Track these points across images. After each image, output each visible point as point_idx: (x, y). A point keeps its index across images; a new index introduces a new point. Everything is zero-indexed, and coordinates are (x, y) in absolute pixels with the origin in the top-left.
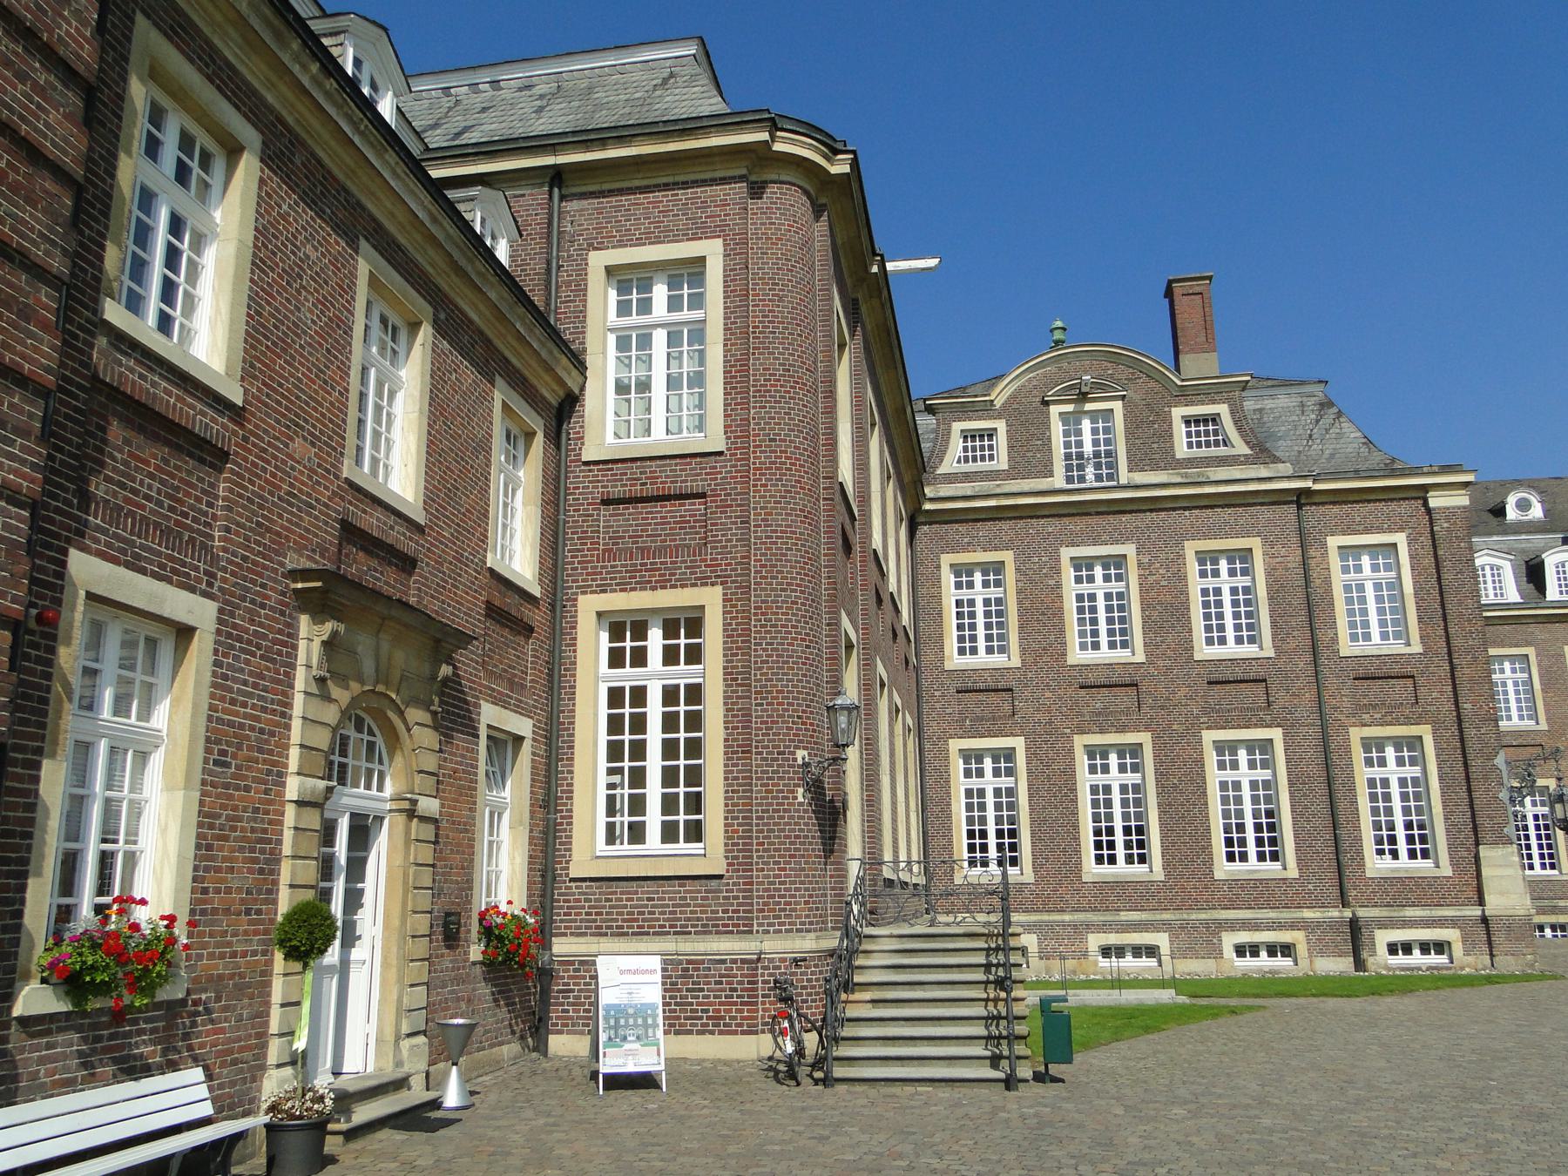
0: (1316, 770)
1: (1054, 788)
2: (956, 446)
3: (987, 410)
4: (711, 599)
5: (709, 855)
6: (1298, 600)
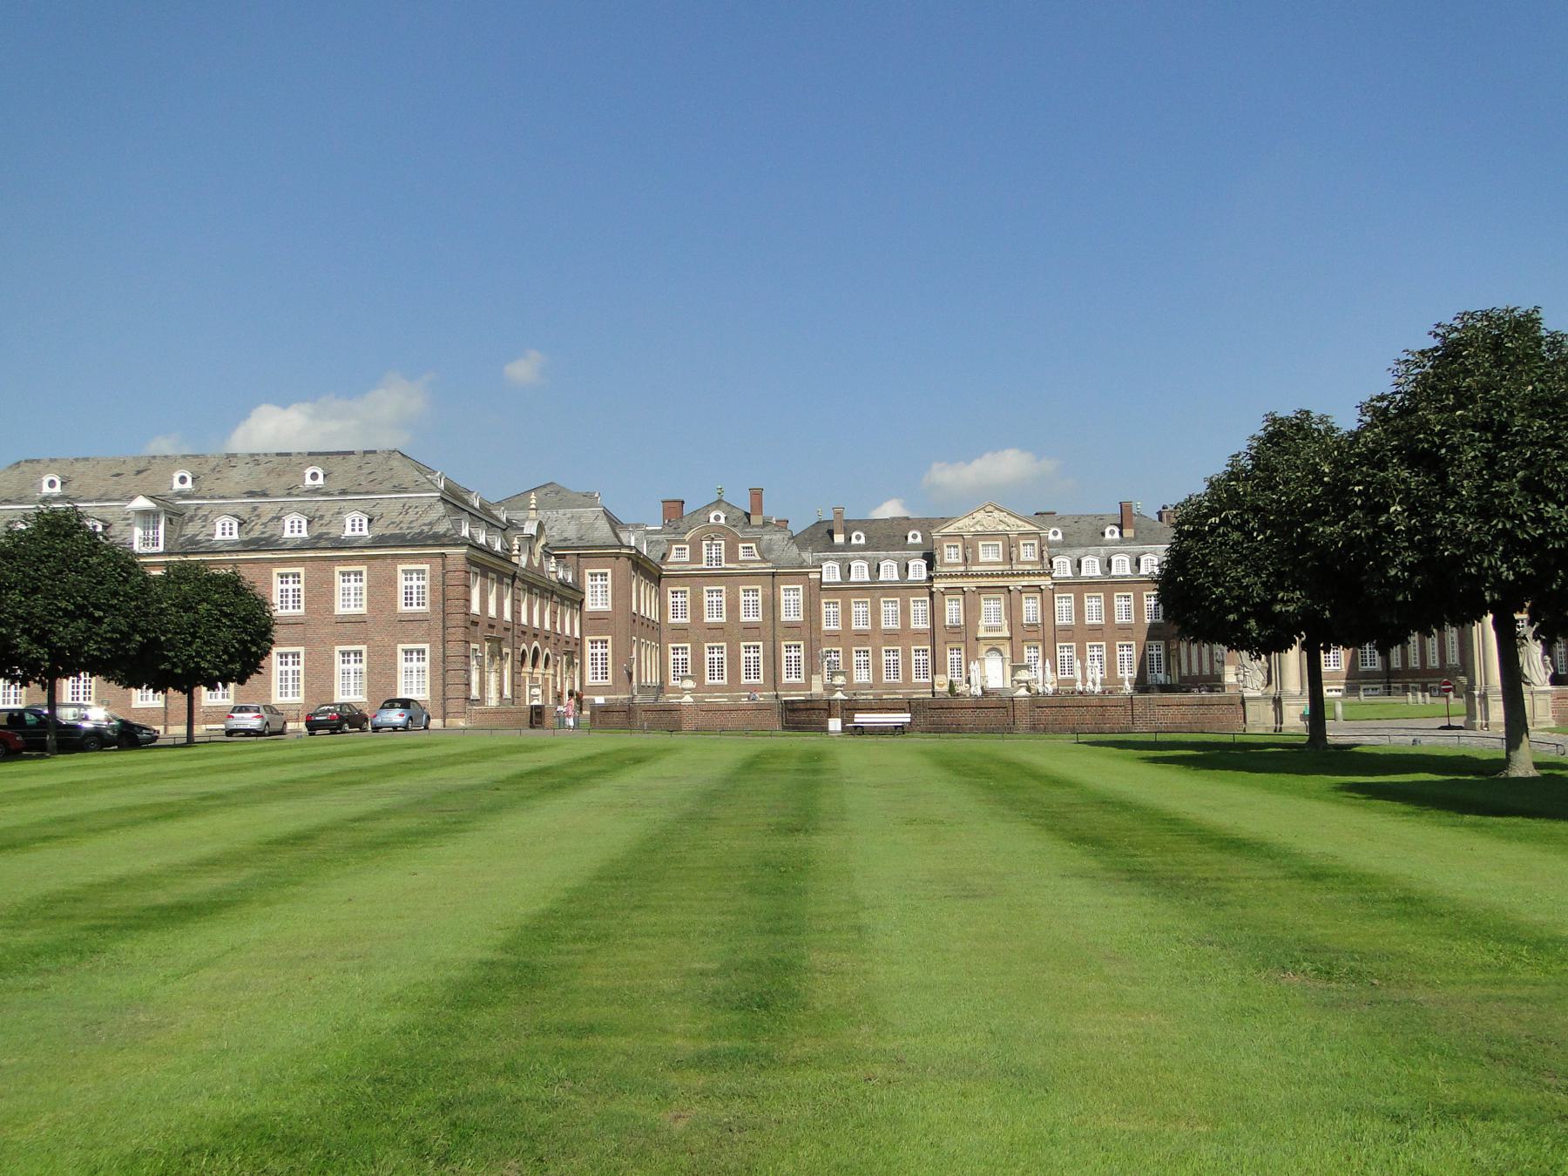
1: (698, 658)
2: (674, 552)
3: (683, 542)
4: (609, 638)
5: (609, 682)
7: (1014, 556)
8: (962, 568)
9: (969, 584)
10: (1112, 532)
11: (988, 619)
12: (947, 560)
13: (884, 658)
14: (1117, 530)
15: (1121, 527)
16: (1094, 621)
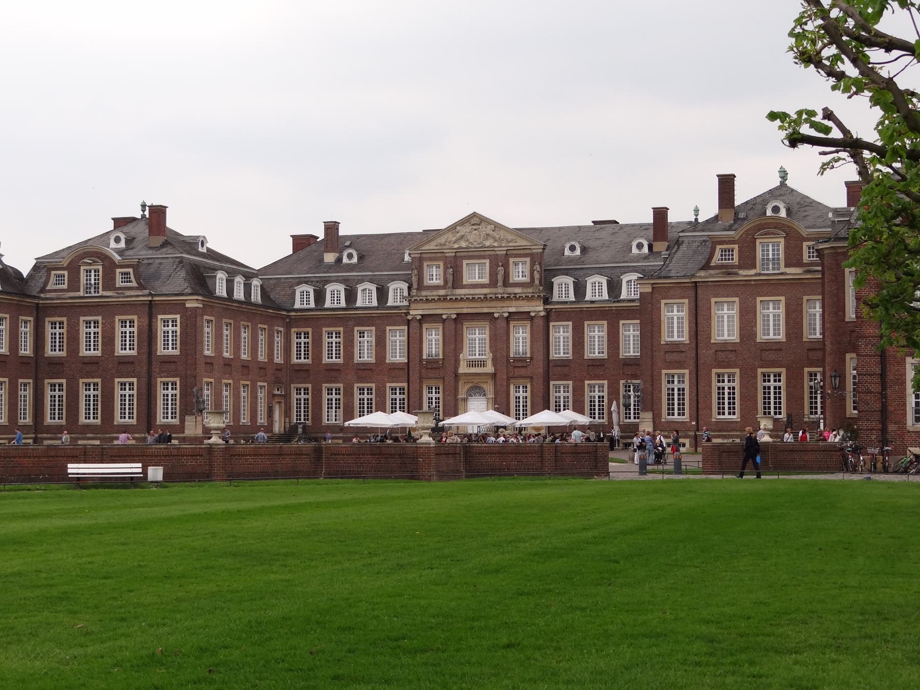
0: (144, 391)
2: (53, 279)
6: (145, 336)
7: (500, 277)
8: (442, 292)
9: (448, 311)
10: (640, 246)
13: (357, 396)
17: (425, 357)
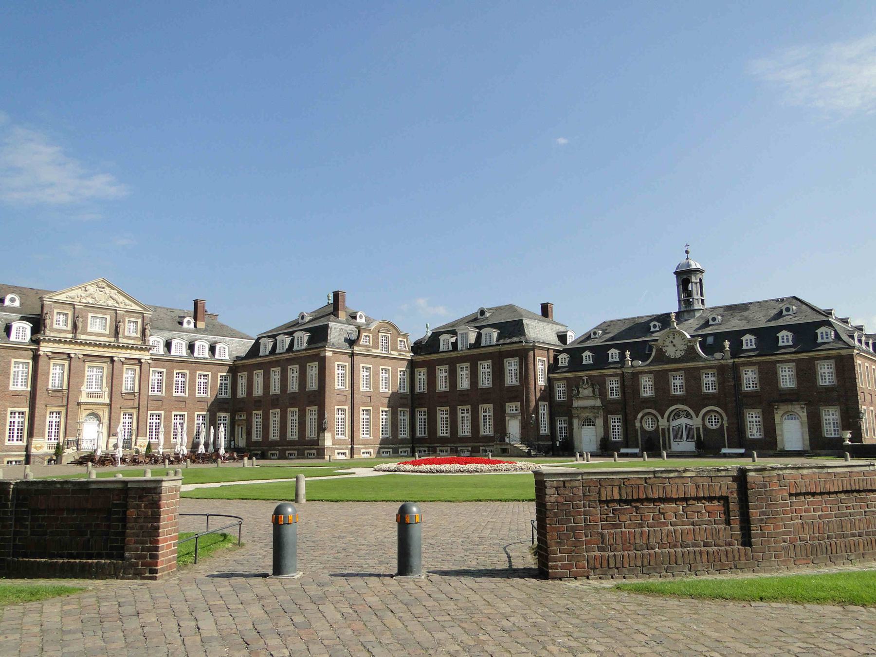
9: (76, 351)
10: (189, 323)
11: (90, 386)
12: (55, 326)
14: (192, 321)
15: (195, 318)
16: (179, 394)
17: (50, 387)
